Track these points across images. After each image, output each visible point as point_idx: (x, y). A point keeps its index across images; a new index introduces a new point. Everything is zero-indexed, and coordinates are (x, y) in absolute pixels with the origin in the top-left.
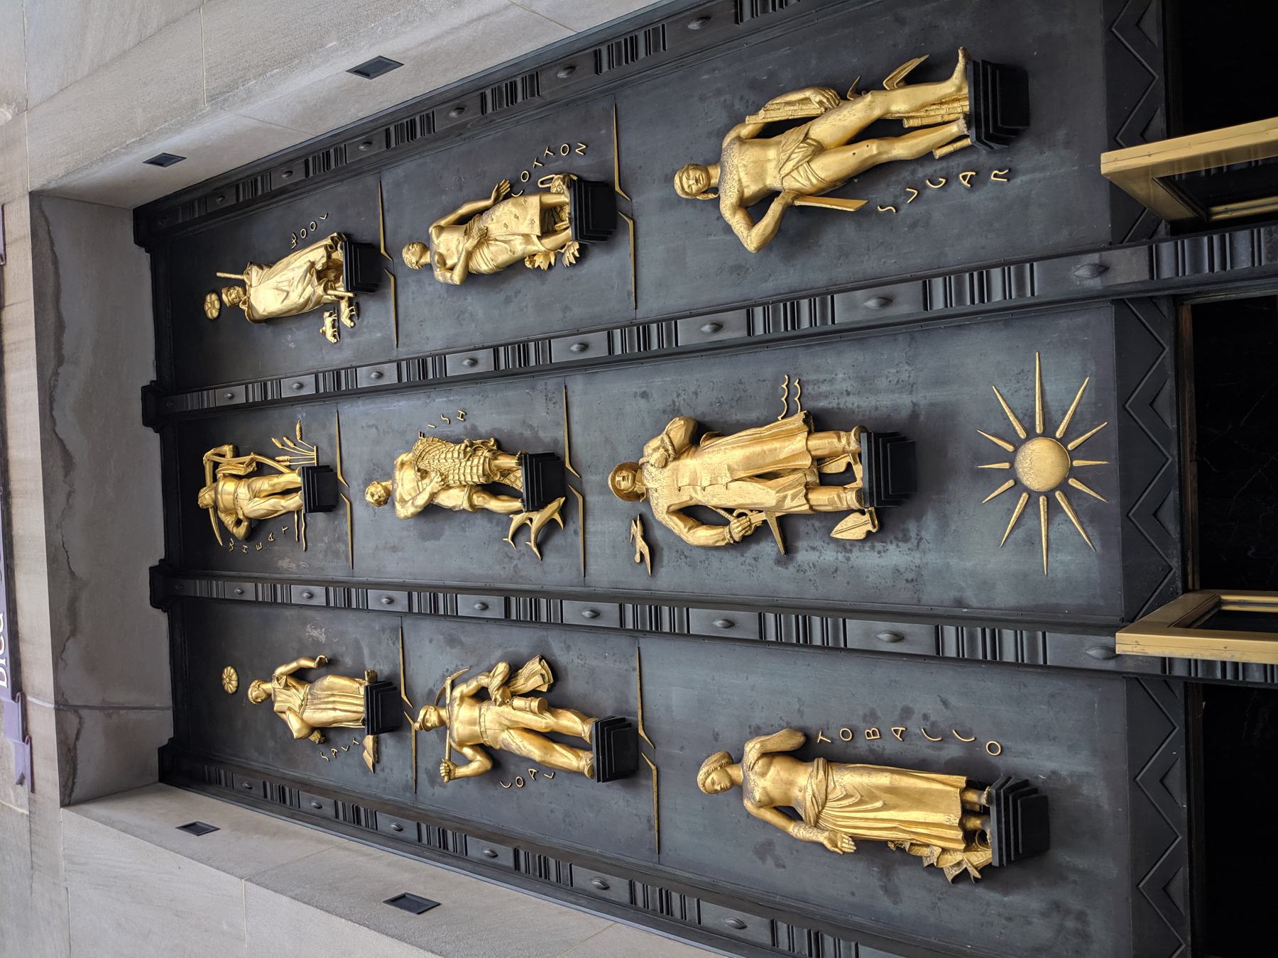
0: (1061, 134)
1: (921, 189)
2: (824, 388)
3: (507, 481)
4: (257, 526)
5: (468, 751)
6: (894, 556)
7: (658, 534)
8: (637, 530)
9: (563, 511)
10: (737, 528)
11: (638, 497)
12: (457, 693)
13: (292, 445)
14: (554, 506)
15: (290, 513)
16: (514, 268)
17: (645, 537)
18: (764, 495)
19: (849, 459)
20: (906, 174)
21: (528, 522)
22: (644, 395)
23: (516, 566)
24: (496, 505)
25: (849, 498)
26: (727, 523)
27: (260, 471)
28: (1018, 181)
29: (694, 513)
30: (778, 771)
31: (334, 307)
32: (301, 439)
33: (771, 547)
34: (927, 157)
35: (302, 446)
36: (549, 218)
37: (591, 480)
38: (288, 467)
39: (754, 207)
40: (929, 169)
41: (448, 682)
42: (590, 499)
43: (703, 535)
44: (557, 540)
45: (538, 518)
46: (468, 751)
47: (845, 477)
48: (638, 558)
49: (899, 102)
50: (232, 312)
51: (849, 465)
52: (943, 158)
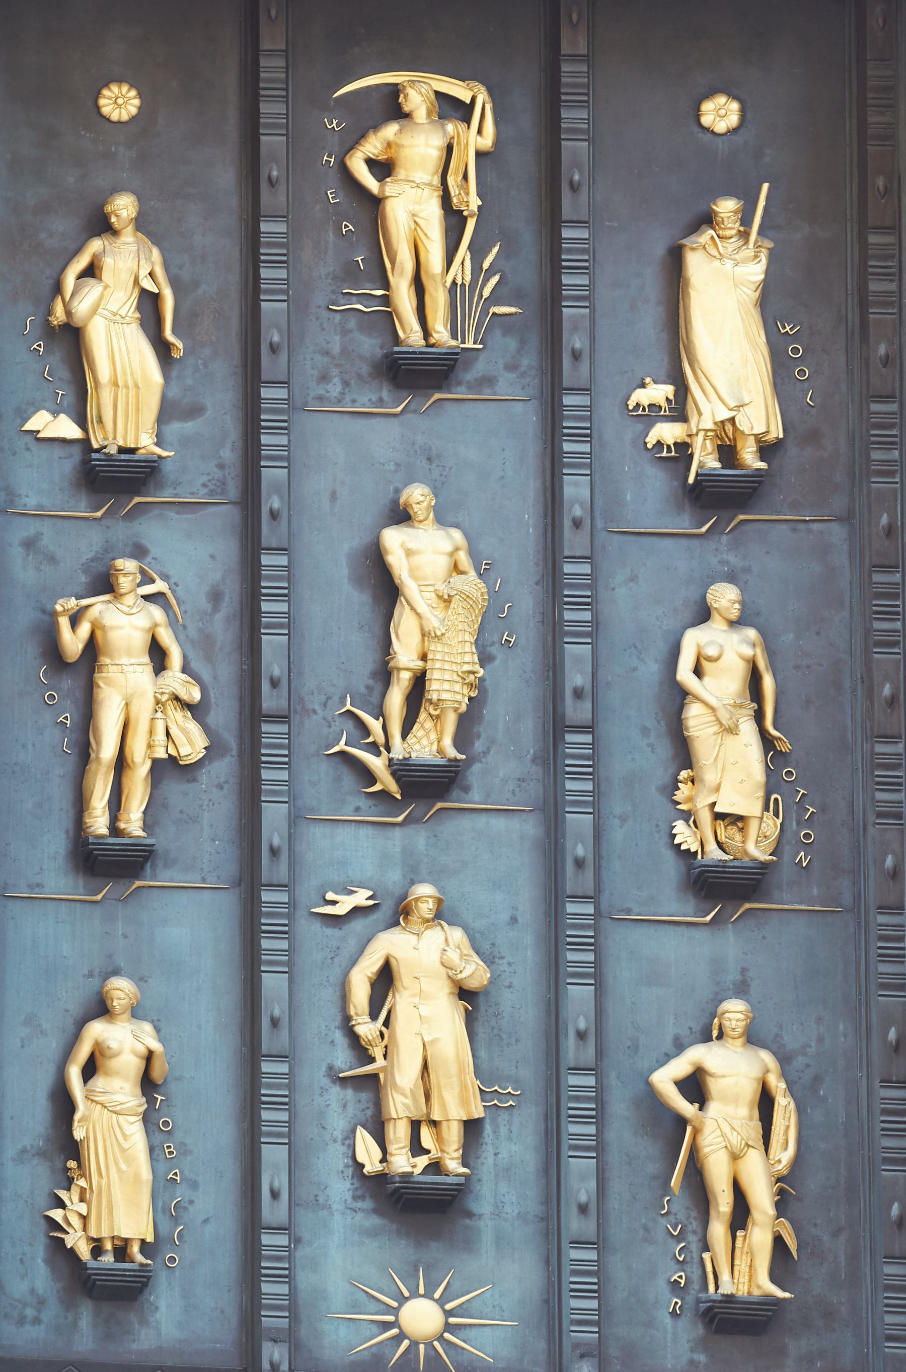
0: (702, 1358)
1: (679, 1239)
2: (503, 1131)
3: (423, 716)
5: (84, 629)
7: (358, 925)
8: (361, 898)
9: (384, 794)
10: (366, 1029)
12: (156, 613)
13: (486, 293)
14: (393, 787)
15: (386, 285)
17: (357, 911)
19: (435, 1154)
20: (695, 1225)
21: (370, 740)
22: (514, 920)
23: (314, 711)
26: (374, 1016)
28: (668, 1320)
32: (494, 314)
35: (485, 311)
37: (419, 837)
38: (454, 283)
40: (695, 1247)
41: (160, 586)
42: (397, 832)
43: (360, 993)
44: (349, 779)
45: (377, 764)
46: (84, 629)
47: (417, 1149)
48: (330, 896)
51: (428, 1152)
52: (702, 1261)
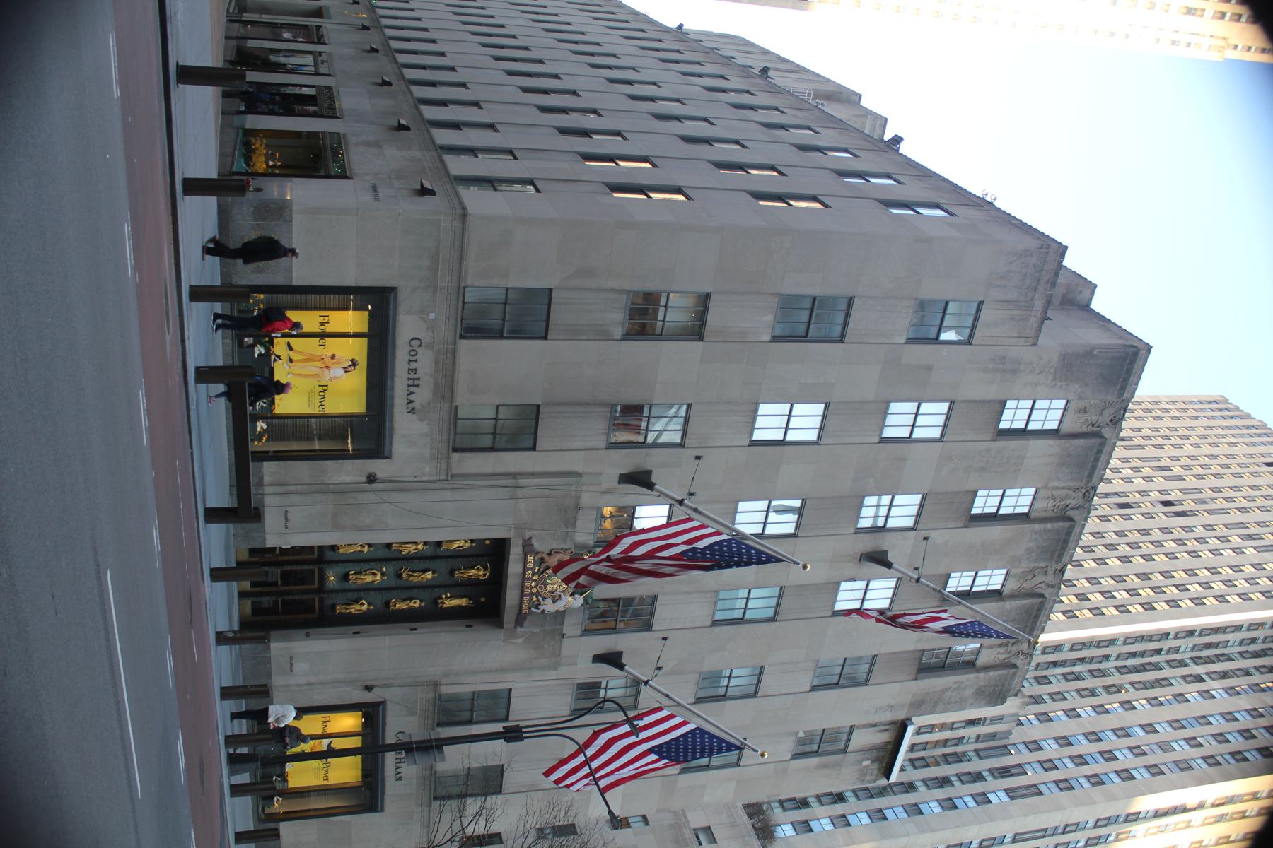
4: (473, 568)
6: (347, 570)
10: (368, 572)
11: (383, 574)
16: (404, 600)
18: (362, 577)
24: (410, 573)
25: (351, 577)
27: (471, 576)
29: (374, 574)
30: (362, 550)
31: (447, 598)
33: (364, 569)
34: (343, 604)
36: (395, 606)
39: (363, 604)
43: (374, 571)
49: (344, 611)
50: (470, 599)
